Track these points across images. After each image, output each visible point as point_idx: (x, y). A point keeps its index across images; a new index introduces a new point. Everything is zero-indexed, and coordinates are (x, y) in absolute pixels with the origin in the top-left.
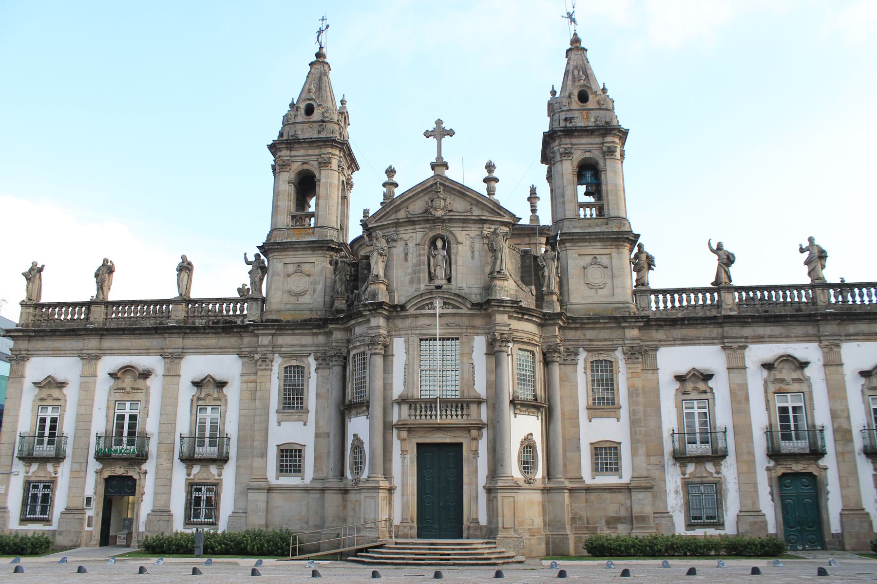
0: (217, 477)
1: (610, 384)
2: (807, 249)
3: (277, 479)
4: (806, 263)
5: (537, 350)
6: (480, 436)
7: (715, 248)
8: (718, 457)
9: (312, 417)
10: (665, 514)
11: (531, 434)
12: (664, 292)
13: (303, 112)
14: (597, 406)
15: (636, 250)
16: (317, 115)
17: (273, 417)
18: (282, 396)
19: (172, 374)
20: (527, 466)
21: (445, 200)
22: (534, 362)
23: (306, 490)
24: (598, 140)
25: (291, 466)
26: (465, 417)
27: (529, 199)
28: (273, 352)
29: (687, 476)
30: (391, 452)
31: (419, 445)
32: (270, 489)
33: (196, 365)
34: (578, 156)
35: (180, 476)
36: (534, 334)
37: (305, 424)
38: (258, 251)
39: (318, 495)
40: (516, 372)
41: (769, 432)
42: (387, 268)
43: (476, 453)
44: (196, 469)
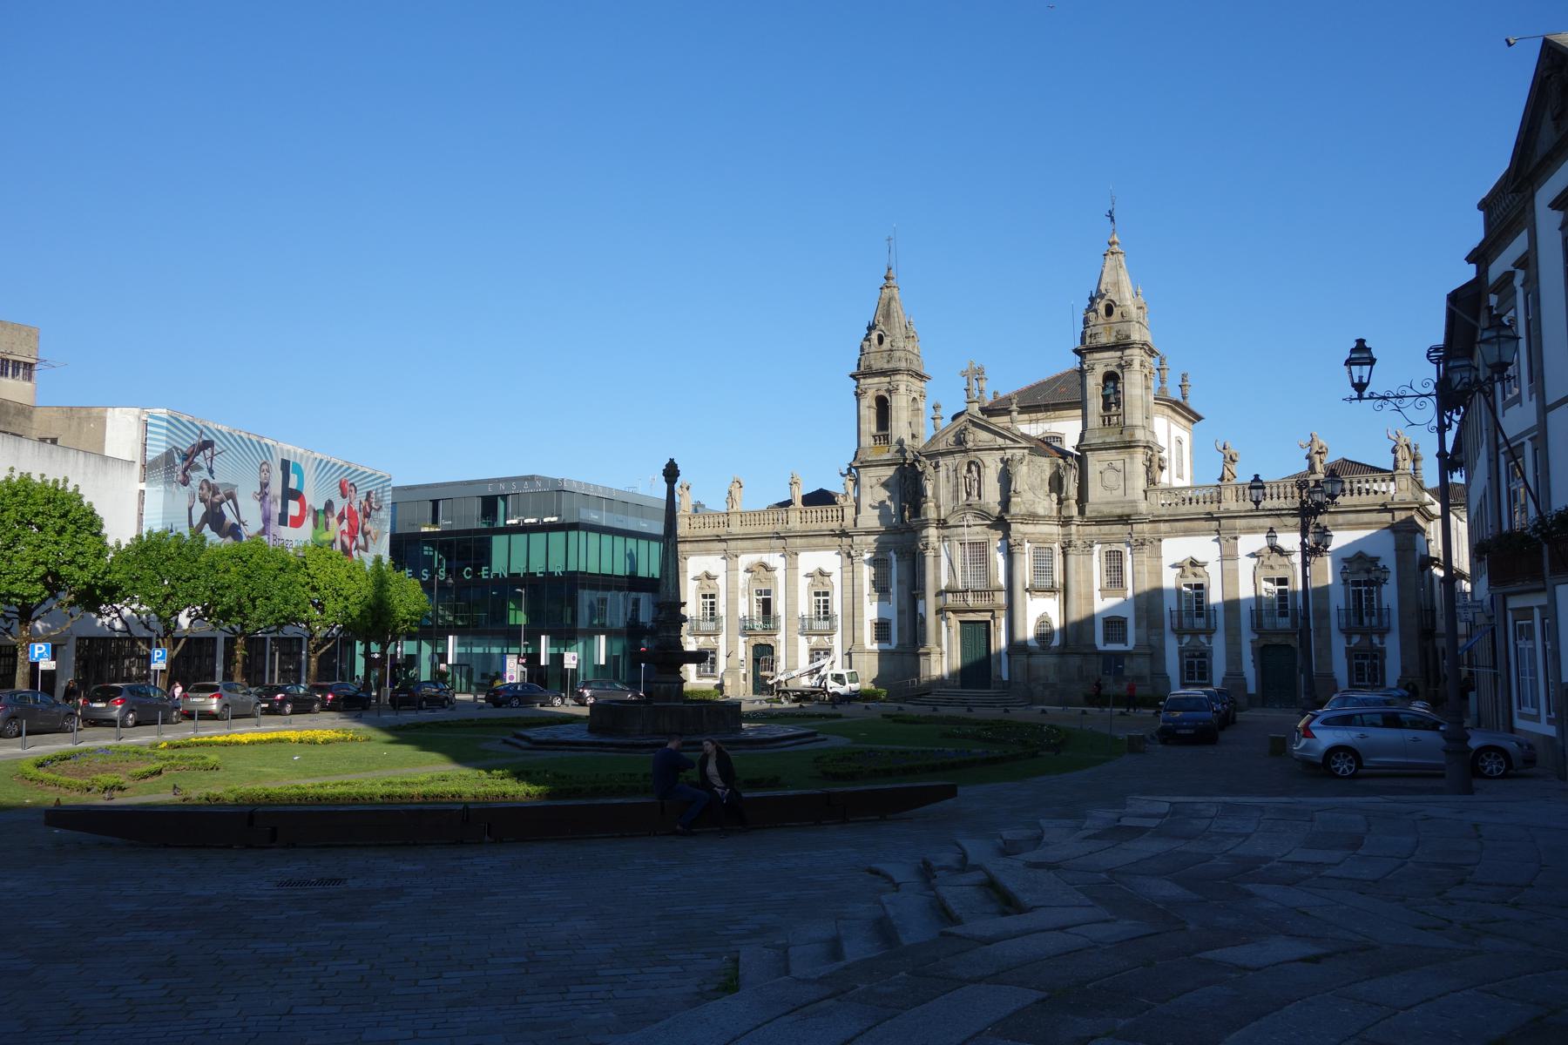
1: (1120, 570)
8: (1209, 632)
16: (886, 344)
19: (791, 568)
24: (1119, 354)
33: (810, 561)
34: (1100, 370)
35: (803, 645)
42: (936, 487)
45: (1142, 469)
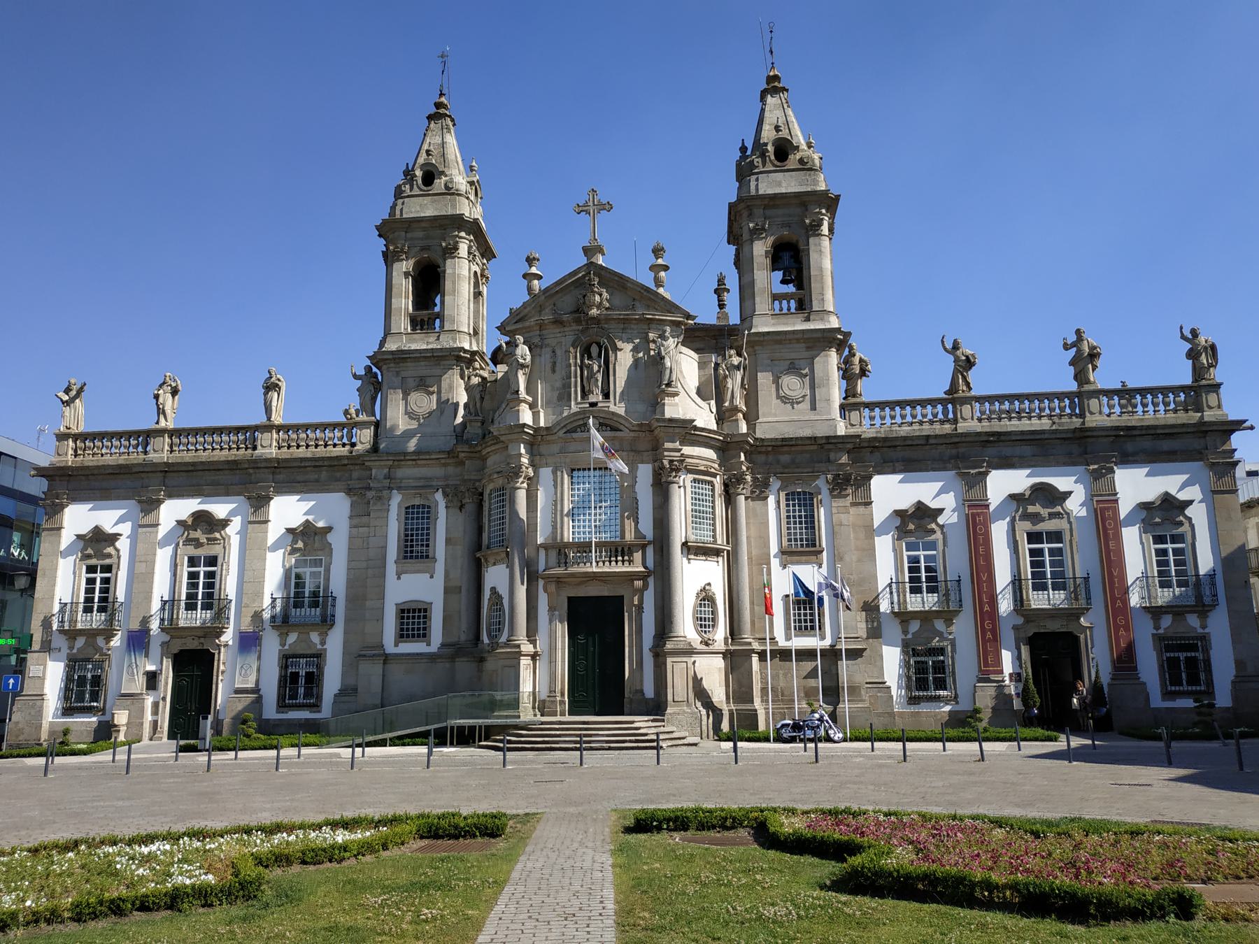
0: (319, 647)
2: (1074, 345)
3: (396, 645)
4: (1072, 363)
5: (718, 481)
6: (646, 587)
7: (949, 346)
9: (440, 567)
10: (881, 685)
11: (709, 584)
12: (882, 405)
13: (420, 182)
14: (794, 549)
15: (846, 352)
16: (439, 184)
17: (391, 568)
18: (403, 543)
20: (705, 623)
21: (601, 295)
22: (713, 496)
23: (431, 658)
25: (413, 629)
26: (626, 563)
27: (716, 291)
28: (391, 489)
29: (910, 636)
30: (536, 608)
31: (569, 598)
32: (387, 658)
36: (713, 461)
37: (432, 577)
38: (368, 363)
39: (448, 665)
40: (689, 507)
41: (1017, 583)
43: (640, 608)
44: (292, 638)
45: (835, 375)
